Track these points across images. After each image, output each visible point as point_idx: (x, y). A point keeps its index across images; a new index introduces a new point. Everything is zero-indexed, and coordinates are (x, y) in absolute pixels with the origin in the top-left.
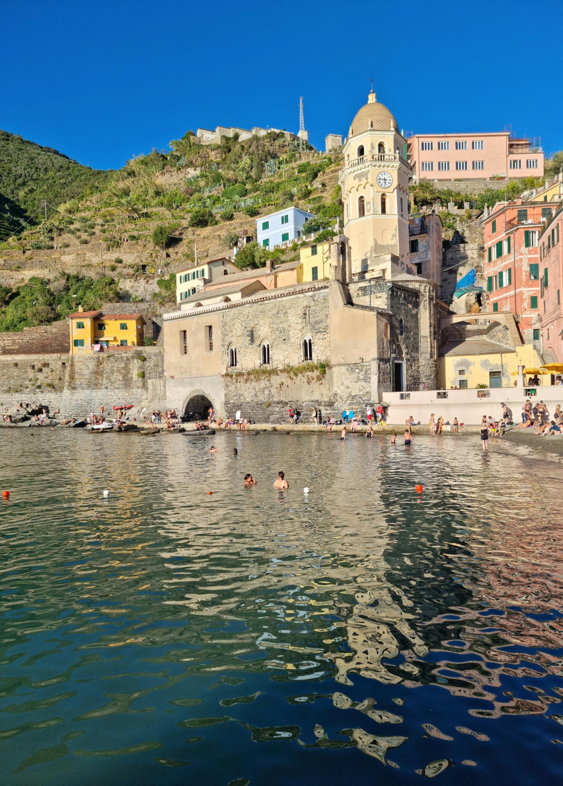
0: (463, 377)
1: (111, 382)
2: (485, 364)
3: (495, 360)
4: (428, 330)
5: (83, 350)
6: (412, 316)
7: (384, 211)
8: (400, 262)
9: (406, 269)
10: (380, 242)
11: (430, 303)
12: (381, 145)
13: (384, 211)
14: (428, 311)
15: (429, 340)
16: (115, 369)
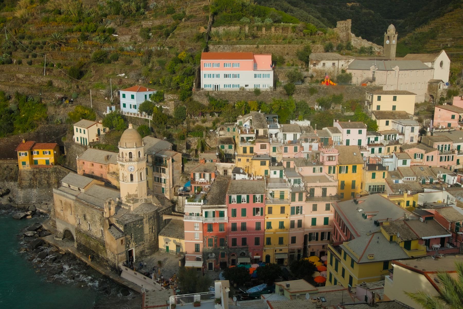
0: (167, 245)
1: (41, 184)
2: (174, 241)
3: (178, 240)
4: (148, 231)
5: (25, 167)
6: (139, 229)
7: (132, 179)
8: (139, 201)
9: (144, 200)
10: (130, 193)
11: (149, 221)
12: (130, 153)
13: (132, 179)
14: (148, 224)
15: (149, 235)
16: (43, 177)
